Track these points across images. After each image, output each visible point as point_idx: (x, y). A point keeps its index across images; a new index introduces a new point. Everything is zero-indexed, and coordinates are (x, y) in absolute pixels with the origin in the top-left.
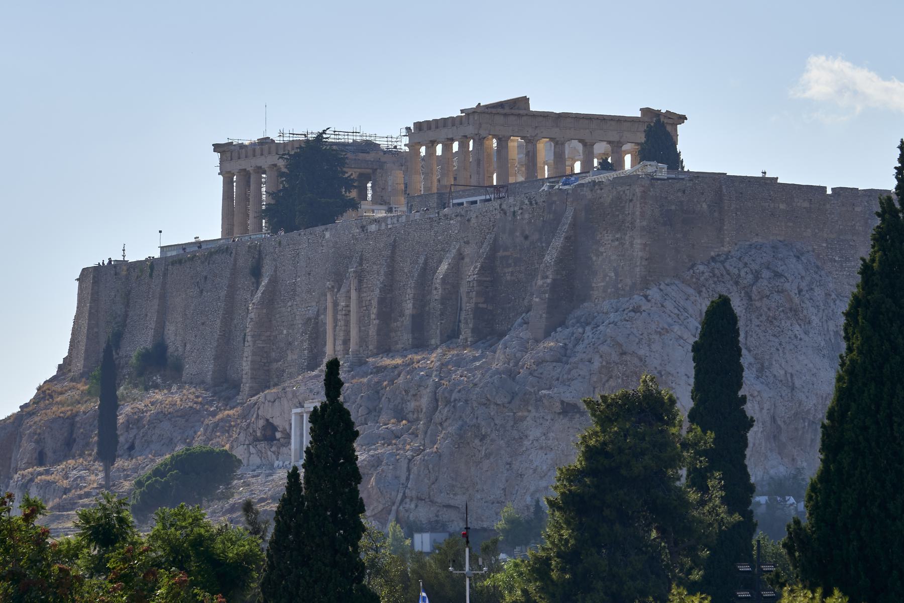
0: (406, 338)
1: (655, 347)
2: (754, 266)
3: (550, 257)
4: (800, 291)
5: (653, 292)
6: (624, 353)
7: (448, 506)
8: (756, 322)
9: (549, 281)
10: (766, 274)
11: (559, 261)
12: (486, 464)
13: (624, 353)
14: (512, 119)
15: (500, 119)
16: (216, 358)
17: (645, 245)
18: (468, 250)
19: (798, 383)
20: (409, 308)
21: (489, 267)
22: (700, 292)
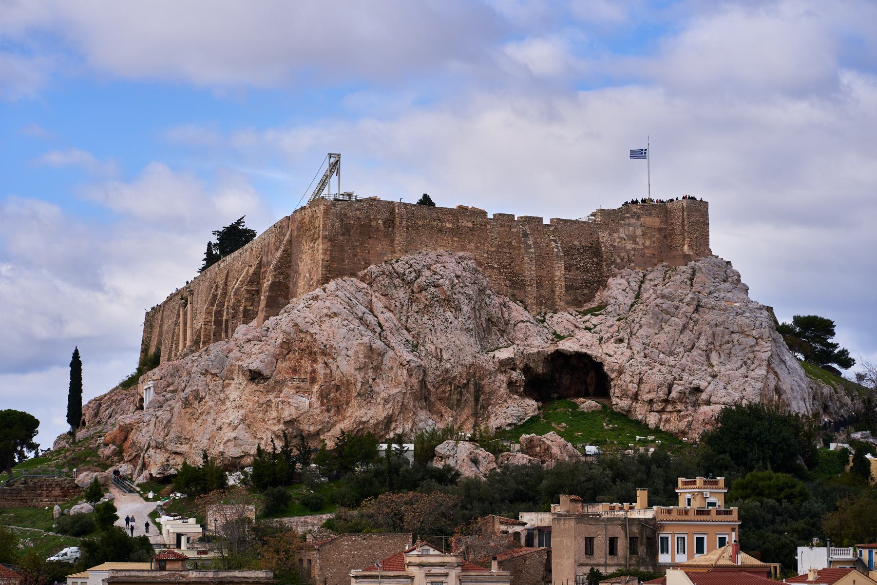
1: (323, 327)
4: (453, 286)
5: (331, 285)
6: (301, 331)
7: (176, 453)
9: (269, 283)
10: (426, 273)
12: (200, 421)
13: (301, 331)
17: (327, 250)
19: (445, 356)
22: (372, 286)
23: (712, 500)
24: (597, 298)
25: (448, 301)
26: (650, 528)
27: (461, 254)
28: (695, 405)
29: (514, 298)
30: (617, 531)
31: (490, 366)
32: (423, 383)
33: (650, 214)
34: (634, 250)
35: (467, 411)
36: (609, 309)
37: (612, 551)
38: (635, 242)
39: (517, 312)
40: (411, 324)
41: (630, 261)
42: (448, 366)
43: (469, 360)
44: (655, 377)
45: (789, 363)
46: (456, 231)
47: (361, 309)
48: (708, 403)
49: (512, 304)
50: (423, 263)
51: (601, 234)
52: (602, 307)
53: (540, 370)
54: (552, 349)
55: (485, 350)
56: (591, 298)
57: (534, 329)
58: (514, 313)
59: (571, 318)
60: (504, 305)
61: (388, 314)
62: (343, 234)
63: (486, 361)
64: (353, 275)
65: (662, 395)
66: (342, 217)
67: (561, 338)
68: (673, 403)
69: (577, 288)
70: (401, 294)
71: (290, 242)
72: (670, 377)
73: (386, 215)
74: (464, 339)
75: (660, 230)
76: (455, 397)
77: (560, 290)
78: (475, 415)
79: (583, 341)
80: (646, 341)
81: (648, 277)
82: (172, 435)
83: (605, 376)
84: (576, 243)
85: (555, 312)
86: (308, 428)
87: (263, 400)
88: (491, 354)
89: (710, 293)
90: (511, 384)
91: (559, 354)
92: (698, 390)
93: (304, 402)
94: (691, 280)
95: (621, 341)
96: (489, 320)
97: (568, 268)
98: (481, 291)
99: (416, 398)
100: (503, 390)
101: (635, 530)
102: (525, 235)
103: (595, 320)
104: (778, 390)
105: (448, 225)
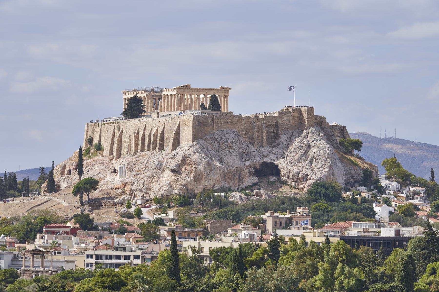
0: (146, 148)
2: (221, 136)
3: (173, 133)
8: (221, 149)
10: (224, 138)
11: (175, 134)
12: (154, 183)
14: (185, 90)
15: (183, 90)
16: (110, 149)
18: (159, 129)
19: (230, 164)
20: (147, 141)
21: (163, 133)
23: (305, 213)
24: (277, 142)
25: (231, 147)
26: (290, 219)
27: (234, 130)
28: (307, 180)
29: (250, 143)
30: (281, 220)
31: (243, 167)
32: (224, 173)
33: (295, 112)
34: (289, 124)
35: (236, 181)
36: (280, 146)
37: (281, 225)
38: (289, 122)
39: (252, 149)
40: (220, 154)
41: (288, 128)
42: (231, 168)
43: (237, 166)
44: (294, 170)
45: (338, 165)
46: (232, 123)
47: (205, 150)
48: (310, 179)
49: (249, 145)
50: (223, 134)
51: (278, 120)
52: (278, 145)
53: (258, 167)
54: (262, 161)
55: (243, 162)
56: (274, 142)
57: (257, 154)
58: (250, 149)
59: (268, 149)
60: (247, 146)
61: (212, 151)
62: (199, 126)
63: (242, 165)
64: (202, 139)
65: (296, 177)
66: (198, 120)
67: (266, 157)
68: (300, 179)
69: (270, 139)
70: (216, 145)
71: (179, 125)
72: (299, 171)
73: (211, 119)
74: (236, 159)
75: (298, 117)
76: (233, 177)
77: (265, 140)
78: (239, 182)
79: (272, 158)
80: (292, 158)
81: (294, 134)
82: (145, 187)
83: (279, 169)
84: (270, 123)
85: (263, 147)
86: (190, 187)
87: (176, 178)
88: (244, 163)
89: (313, 141)
90: (250, 173)
91: (264, 162)
92: (307, 175)
93: (188, 179)
94: (308, 136)
95: (284, 158)
96: (242, 152)
97: (267, 132)
98: (240, 142)
99: (222, 178)
100: (248, 175)
101: (286, 220)
102: (254, 122)
103: (276, 150)
104: (333, 175)
105: (230, 121)
